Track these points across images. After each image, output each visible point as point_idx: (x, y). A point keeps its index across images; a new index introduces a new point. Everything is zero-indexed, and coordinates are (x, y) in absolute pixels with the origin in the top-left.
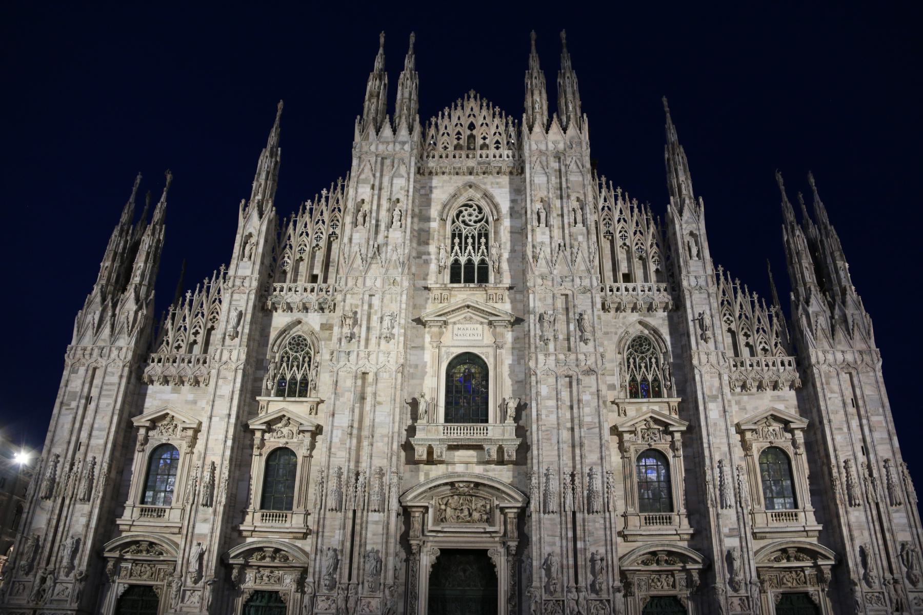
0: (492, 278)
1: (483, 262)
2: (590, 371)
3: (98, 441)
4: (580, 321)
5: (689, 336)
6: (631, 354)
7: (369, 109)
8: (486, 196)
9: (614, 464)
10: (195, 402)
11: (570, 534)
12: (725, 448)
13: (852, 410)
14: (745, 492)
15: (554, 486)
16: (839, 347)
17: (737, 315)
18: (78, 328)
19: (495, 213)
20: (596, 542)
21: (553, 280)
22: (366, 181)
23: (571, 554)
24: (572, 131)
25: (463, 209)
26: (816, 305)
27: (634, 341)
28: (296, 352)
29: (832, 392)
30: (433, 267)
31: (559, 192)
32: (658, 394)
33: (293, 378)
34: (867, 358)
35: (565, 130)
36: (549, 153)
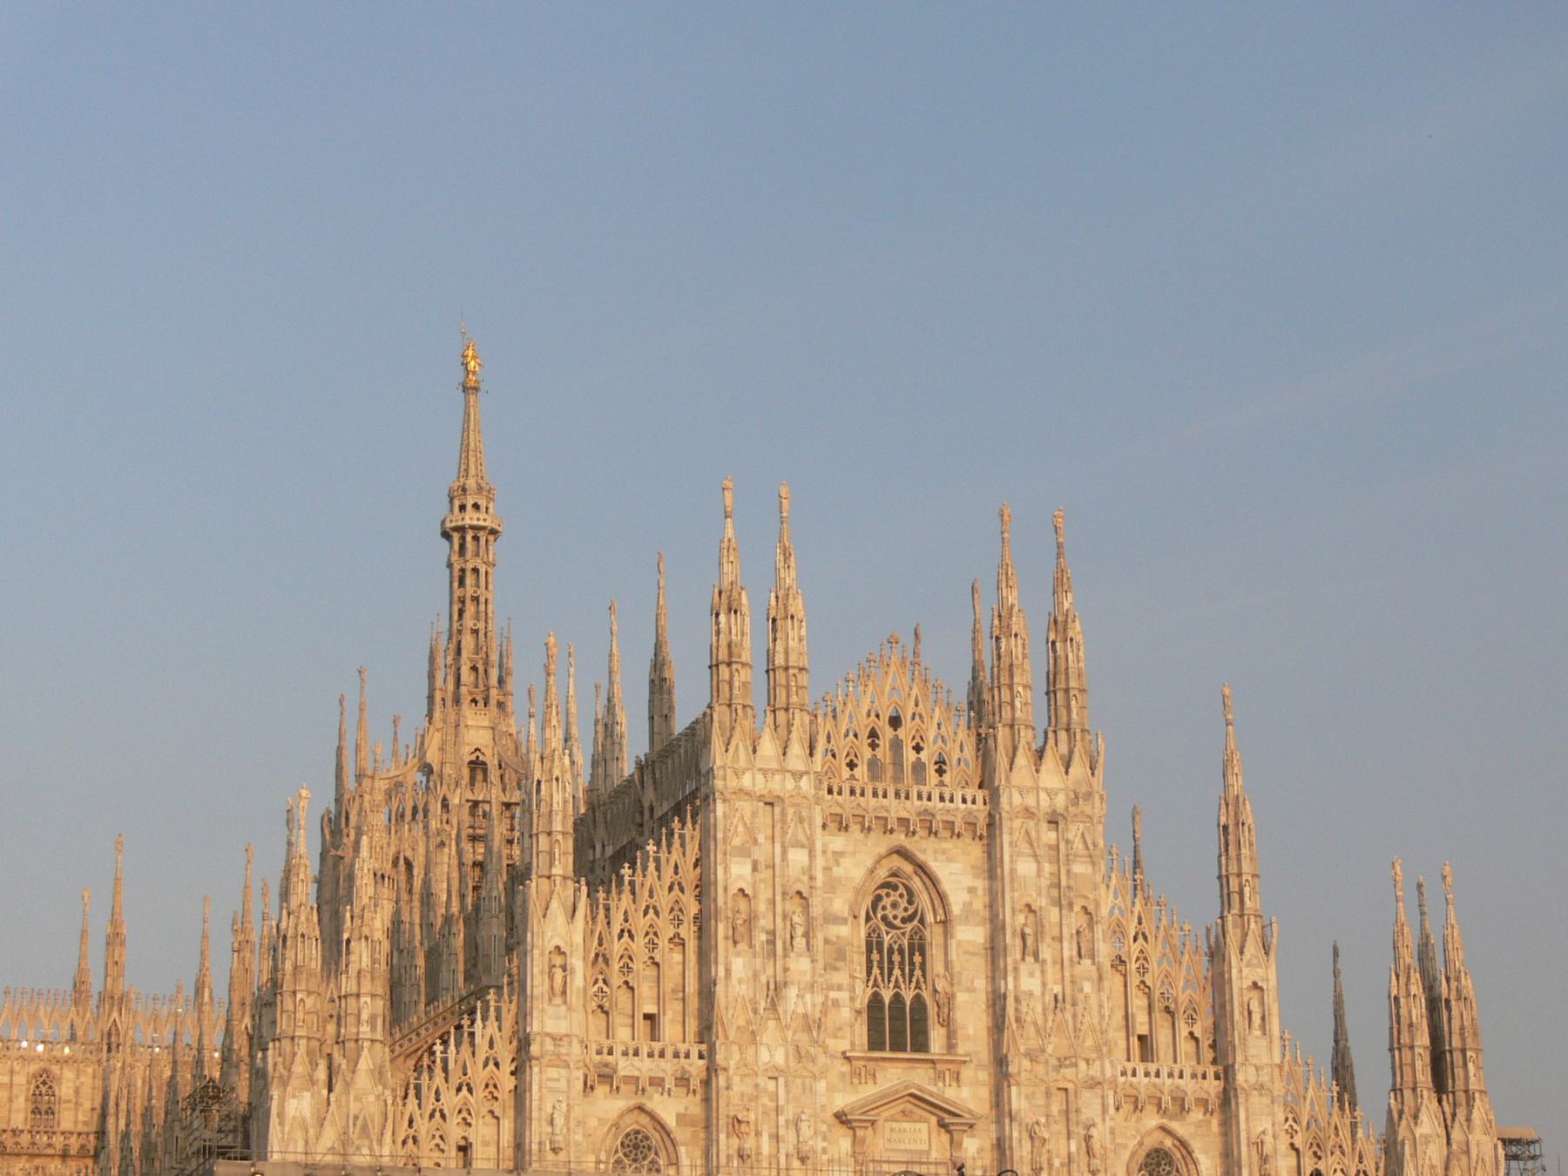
0: (937, 1037)
1: (918, 999)
4: (1088, 1138)
7: (731, 684)
17: (1304, 1124)
18: (282, 1124)
19: (940, 911)
21: (1047, 1063)
22: (743, 852)
24: (1078, 769)
25: (883, 892)
26: (1428, 1124)
27: (1148, 1156)
28: (635, 1160)
30: (846, 1013)
31: (1055, 892)
36: (1041, 815)
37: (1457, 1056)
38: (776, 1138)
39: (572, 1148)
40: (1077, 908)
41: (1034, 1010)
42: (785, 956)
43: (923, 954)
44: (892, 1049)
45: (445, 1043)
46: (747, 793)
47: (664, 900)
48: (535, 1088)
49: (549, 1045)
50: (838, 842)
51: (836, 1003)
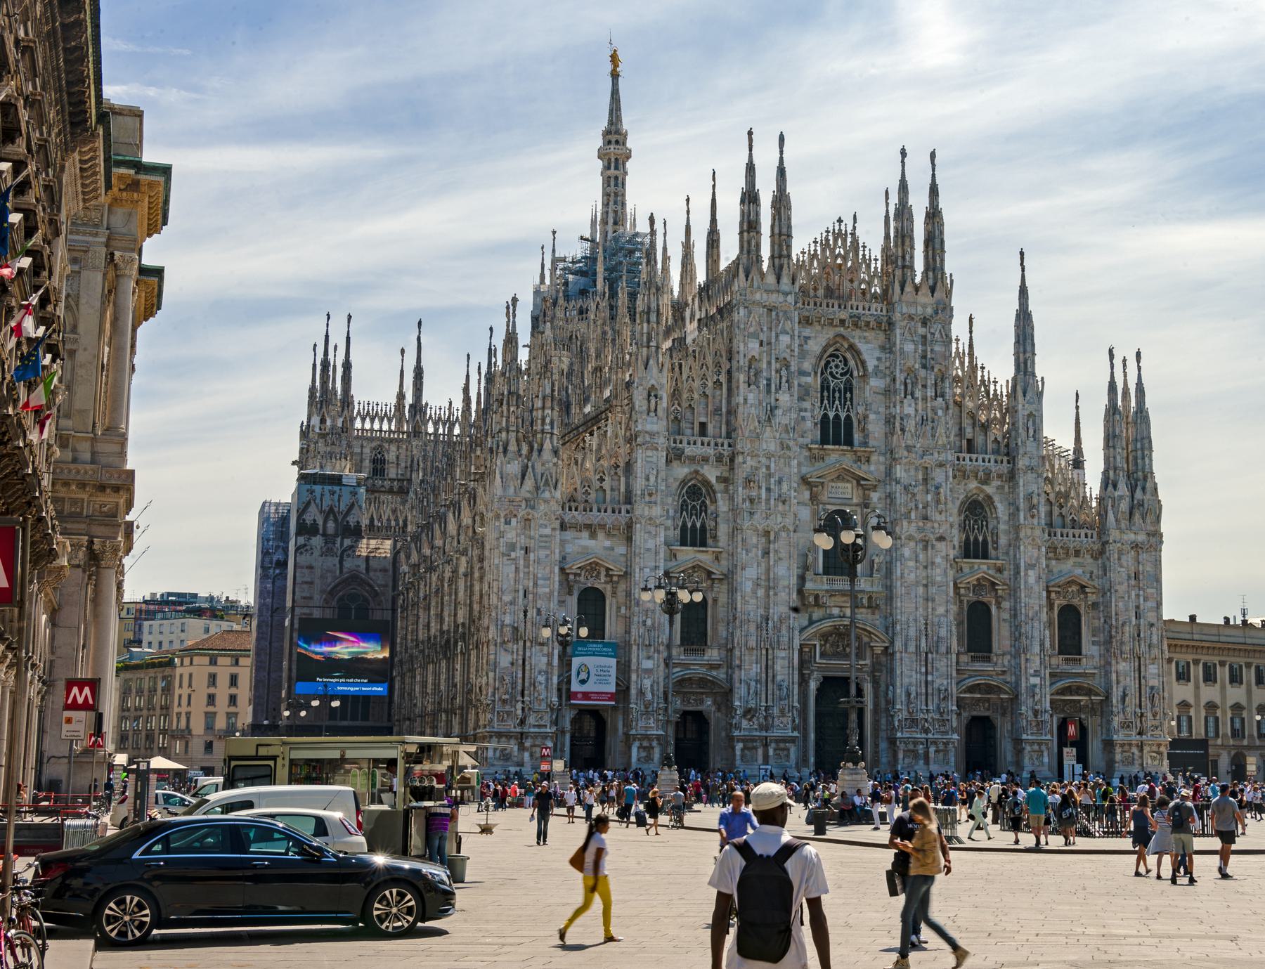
0: (857, 437)
1: (848, 418)
2: (941, 539)
3: (543, 590)
5: (1018, 509)
8: (852, 347)
10: (612, 549)
11: (923, 670)
13: (1133, 582)
14: (1047, 644)
15: (912, 633)
20: (941, 676)
26: (1123, 489)
29: (1121, 566)
30: (809, 424)
32: (985, 556)
33: (694, 525)
34: (1153, 540)
35: (933, 290)
36: (917, 319)
37: (1139, 453)
38: (768, 490)
41: (911, 425)
42: (777, 392)
43: (851, 393)
44: (834, 444)
45: (591, 434)
46: (759, 304)
47: (709, 361)
48: (639, 461)
50: (807, 332)
51: (803, 418)
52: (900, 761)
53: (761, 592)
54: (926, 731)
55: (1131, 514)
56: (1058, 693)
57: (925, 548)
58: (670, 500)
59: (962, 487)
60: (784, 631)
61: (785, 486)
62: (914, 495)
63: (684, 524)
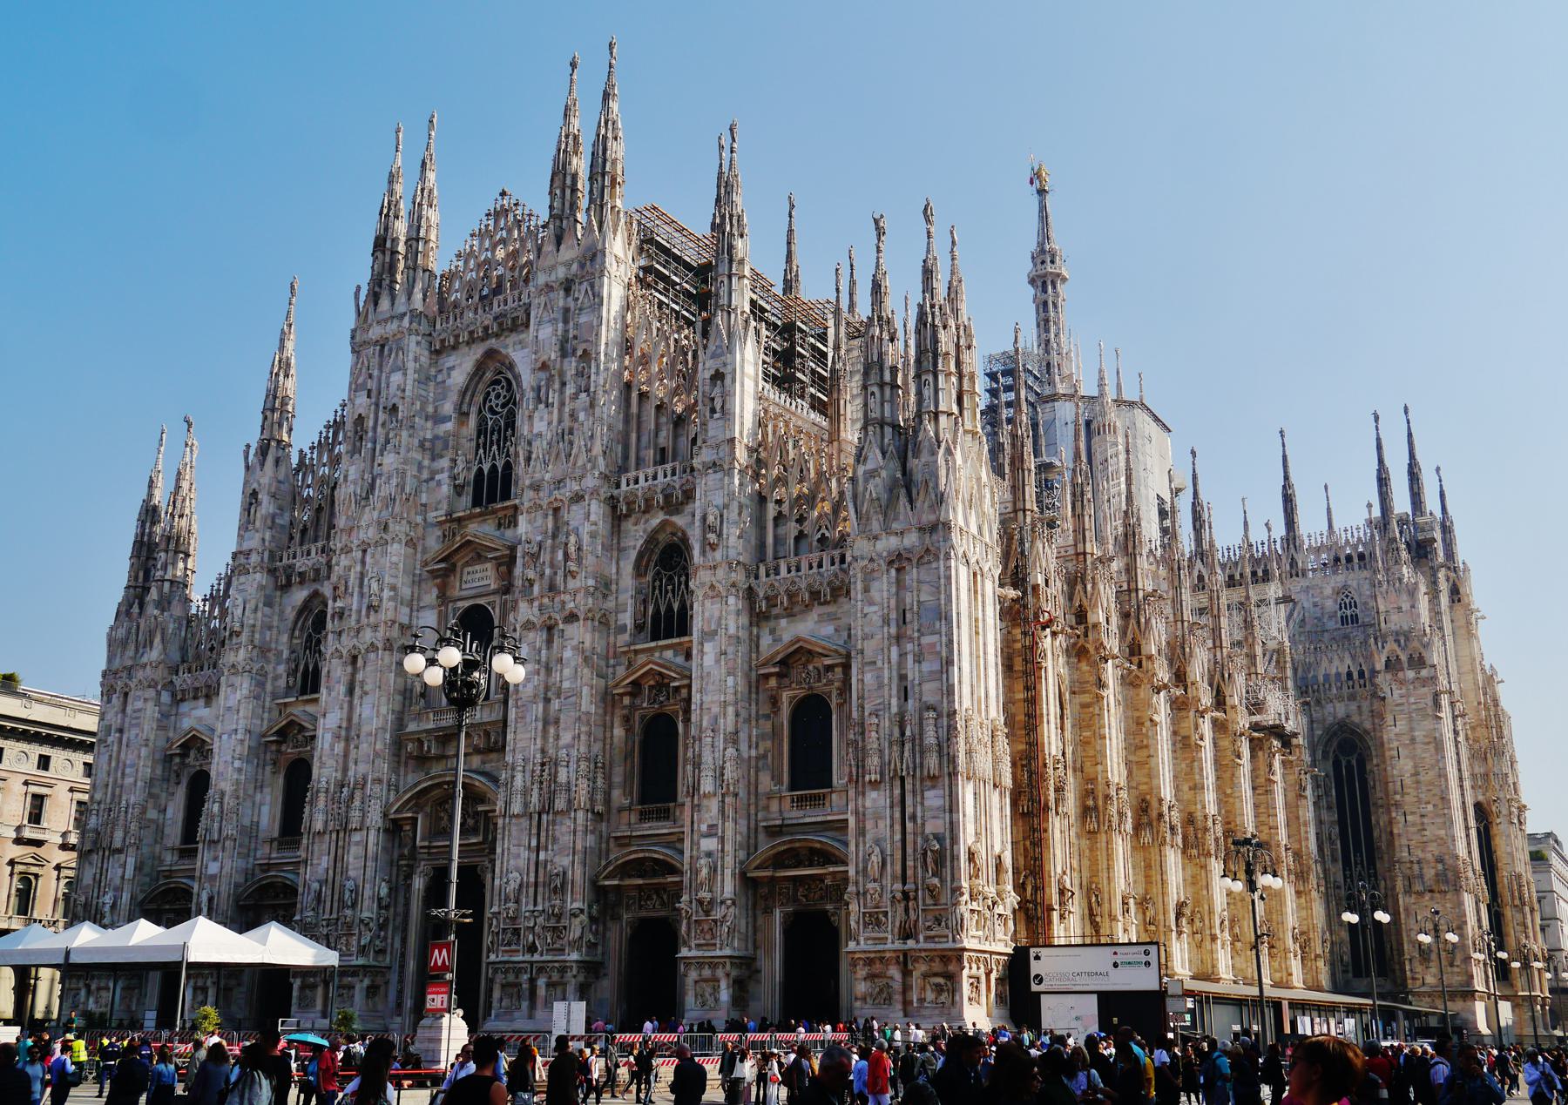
2: (572, 618)
6: (658, 573)
9: (616, 740)
11: (534, 843)
12: (715, 709)
14: (729, 774)
16: (896, 526)
20: (561, 852)
23: (532, 868)
27: (663, 552)
29: (871, 603)
30: (445, 489)
39: (246, 630)
40: (579, 353)
41: (539, 447)
49: (242, 560)
50: (450, 360)
52: (495, 1004)
53: (339, 748)
54: (532, 949)
55: (889, 500)
56: (778, 861)
57: (550, 641)
58: (285, 638)
59: (641, 527)
60: (357, 803)
61: (375, 586)
62: (535, 557)
63: (306, 666)
